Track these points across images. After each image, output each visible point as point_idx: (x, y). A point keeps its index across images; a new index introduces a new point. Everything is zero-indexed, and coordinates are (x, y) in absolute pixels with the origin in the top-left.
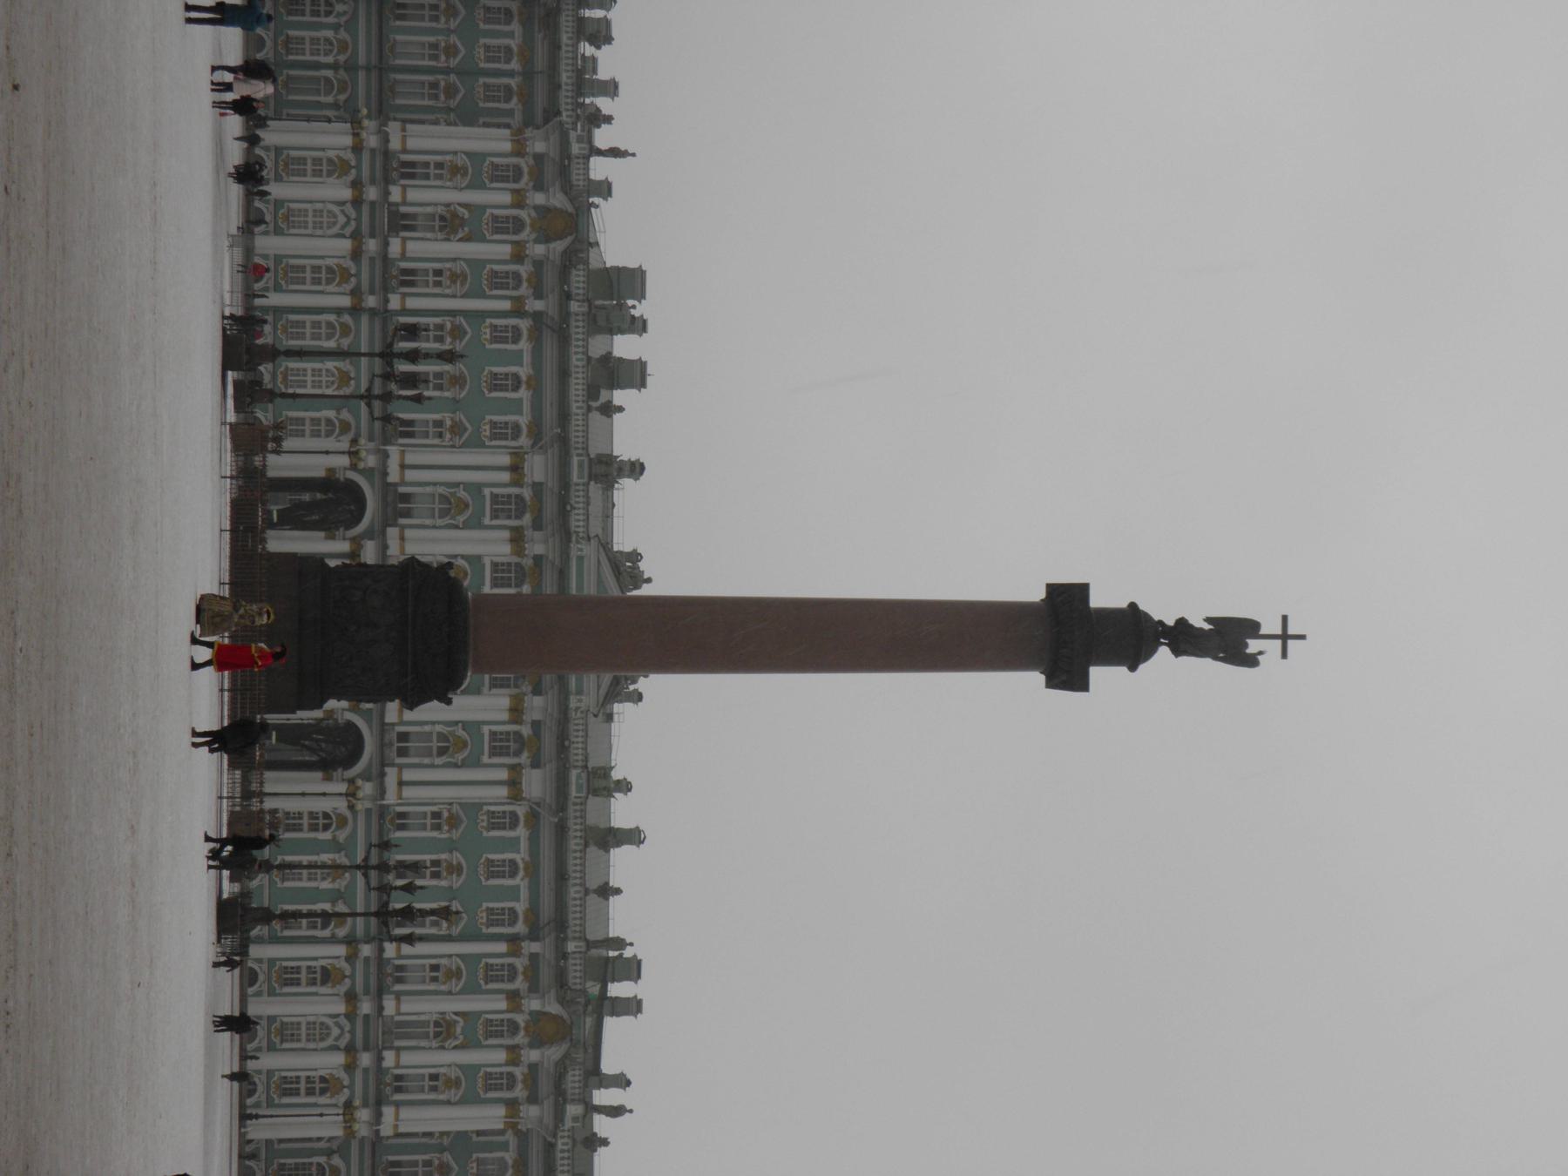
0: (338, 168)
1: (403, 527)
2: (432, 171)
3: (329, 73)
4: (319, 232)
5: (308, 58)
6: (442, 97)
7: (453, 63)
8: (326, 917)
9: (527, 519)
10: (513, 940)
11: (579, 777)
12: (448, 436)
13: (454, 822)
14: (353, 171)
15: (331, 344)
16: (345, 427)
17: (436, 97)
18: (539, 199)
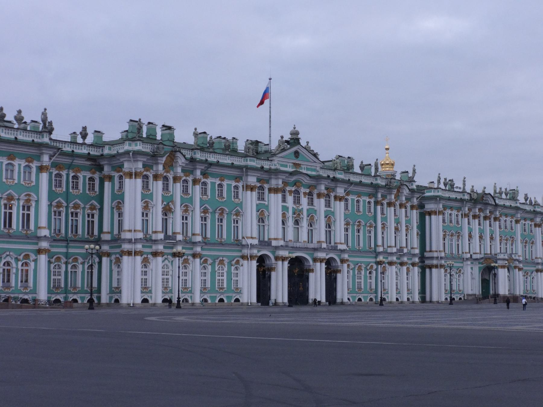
0: (145, 263)
1: (269, 239)
2: (145, 218)
3: (70, 266)
4: (170, 273)
5: (62, 278)
6: (78, 210)
7: (65, 204)
8: (370, 273)
9: (266, 186)
10: (376, 203)
11: (339, 174)
12: (239, 217)
13: (347, 224)
14: (149, 256)
15: (210, 267)
16: (238, 262)
17: (77, 214)
18: (161, 167)
